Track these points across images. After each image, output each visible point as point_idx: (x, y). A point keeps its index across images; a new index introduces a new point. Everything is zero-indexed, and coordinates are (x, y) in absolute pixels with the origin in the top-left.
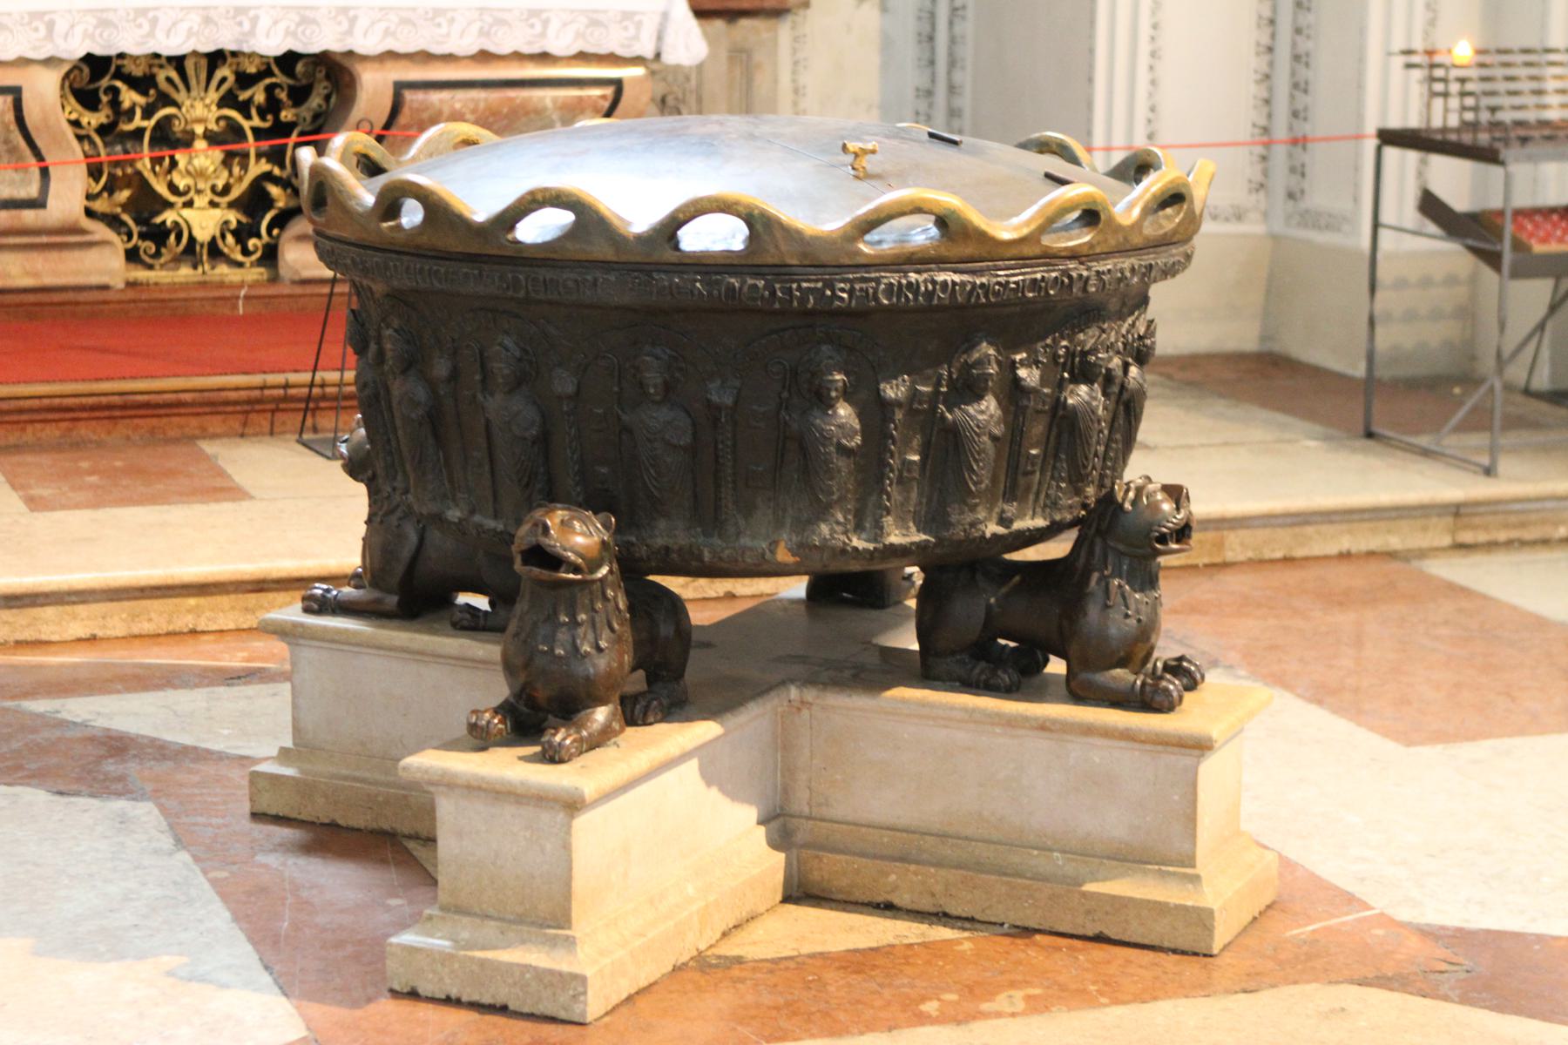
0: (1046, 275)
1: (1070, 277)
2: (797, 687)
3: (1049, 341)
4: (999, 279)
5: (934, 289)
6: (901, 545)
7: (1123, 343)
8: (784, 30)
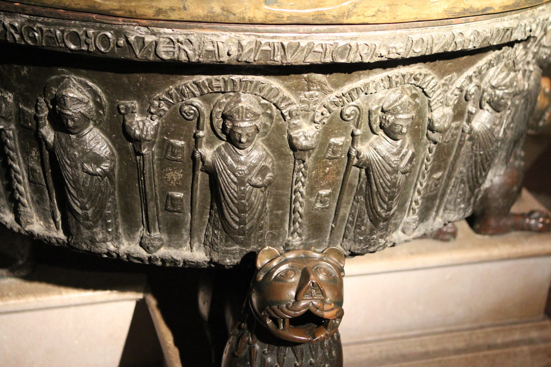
4: (31, 25)
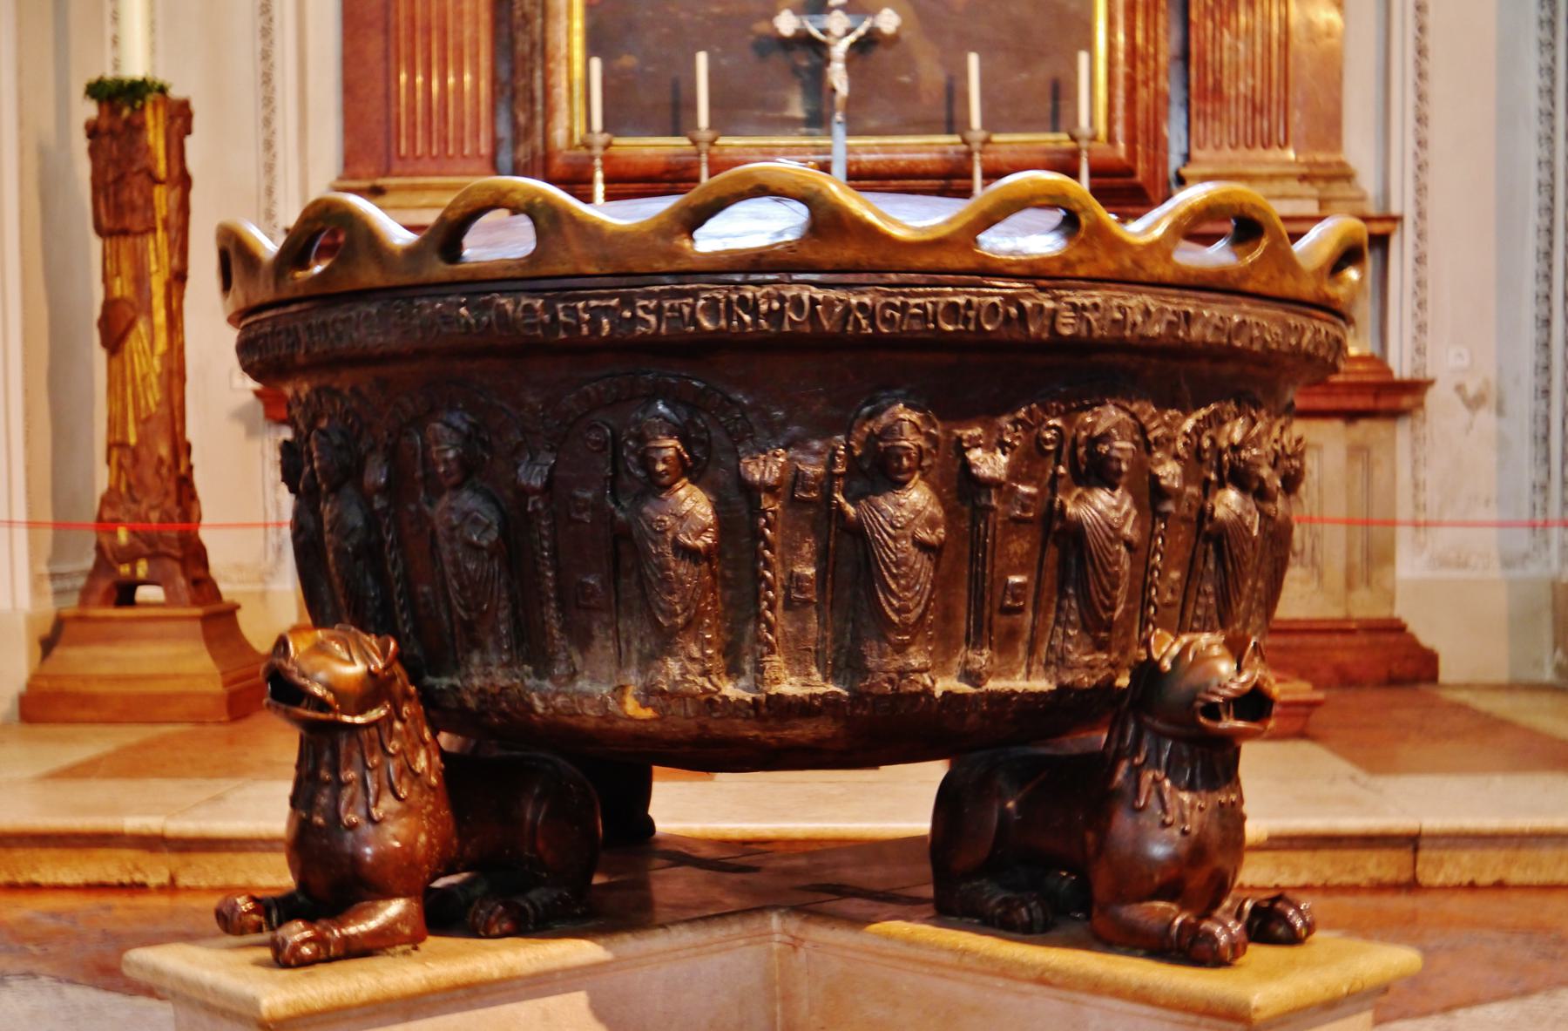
0: (975, 299)
1: (1021, 307)
2: (781, 915)
3: (1022, 414)
4: (892, 300)
5: (782, 308)
6: (795, 696)
7: (1185, 444)
8: (1402, 431)
